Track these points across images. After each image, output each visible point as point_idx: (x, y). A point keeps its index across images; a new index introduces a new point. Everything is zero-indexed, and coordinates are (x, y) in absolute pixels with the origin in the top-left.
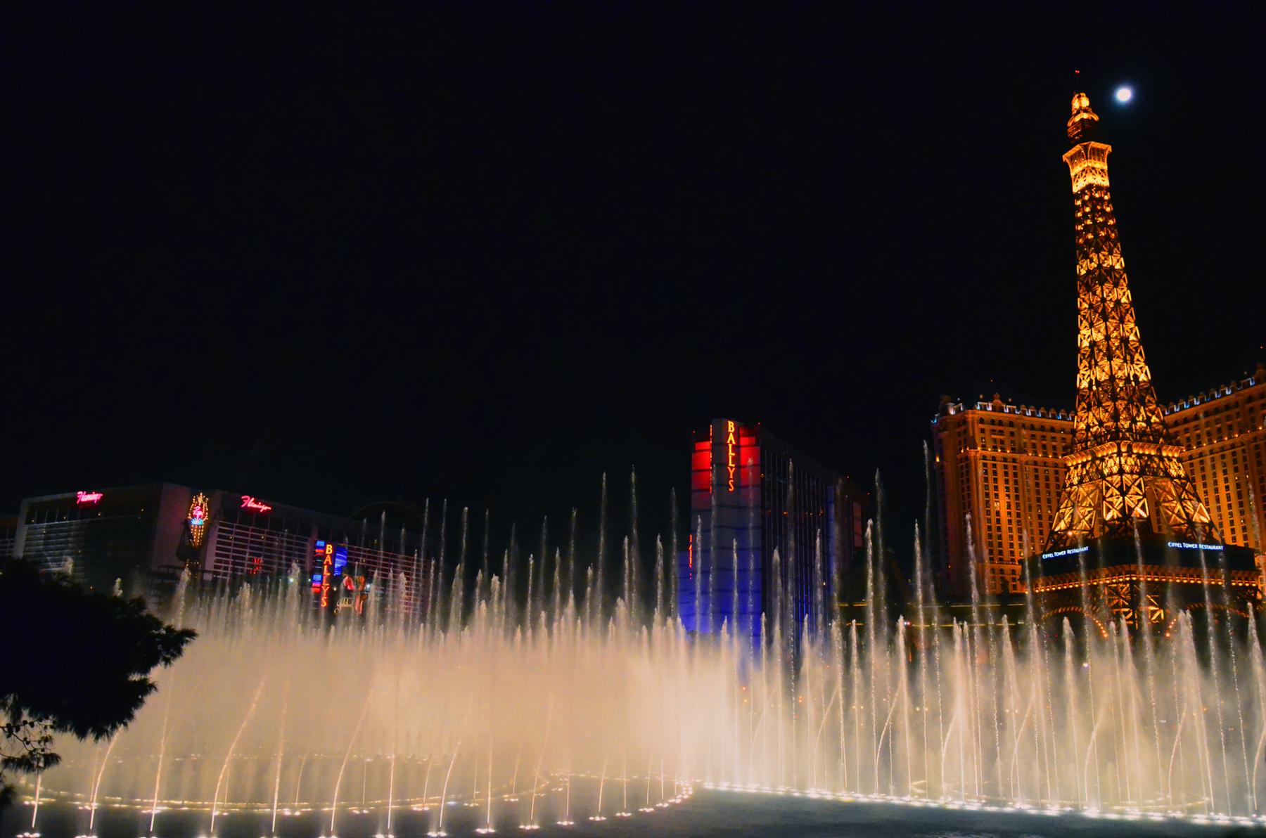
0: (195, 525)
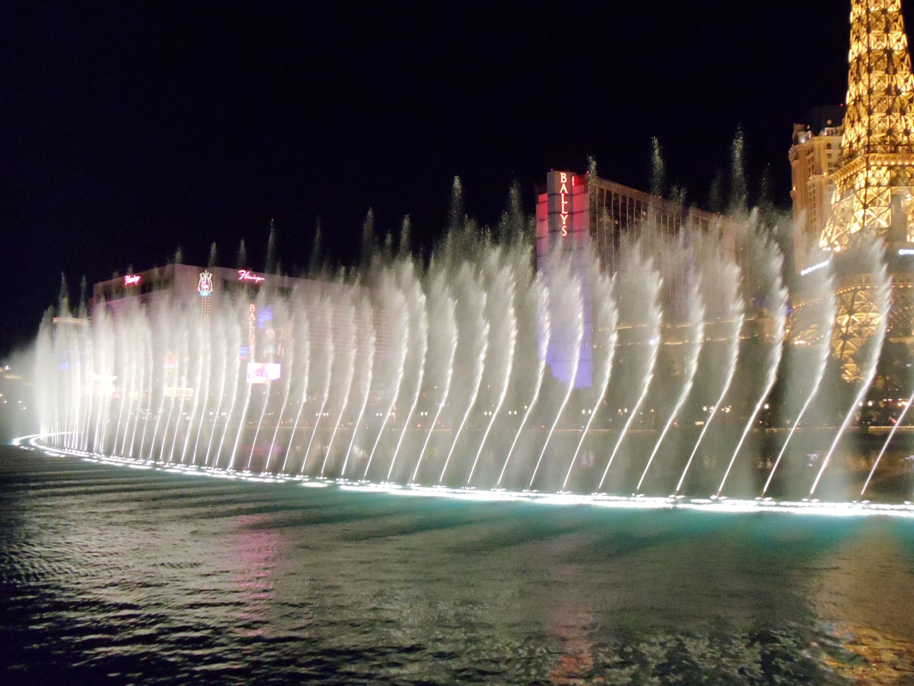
0: (204, 297)
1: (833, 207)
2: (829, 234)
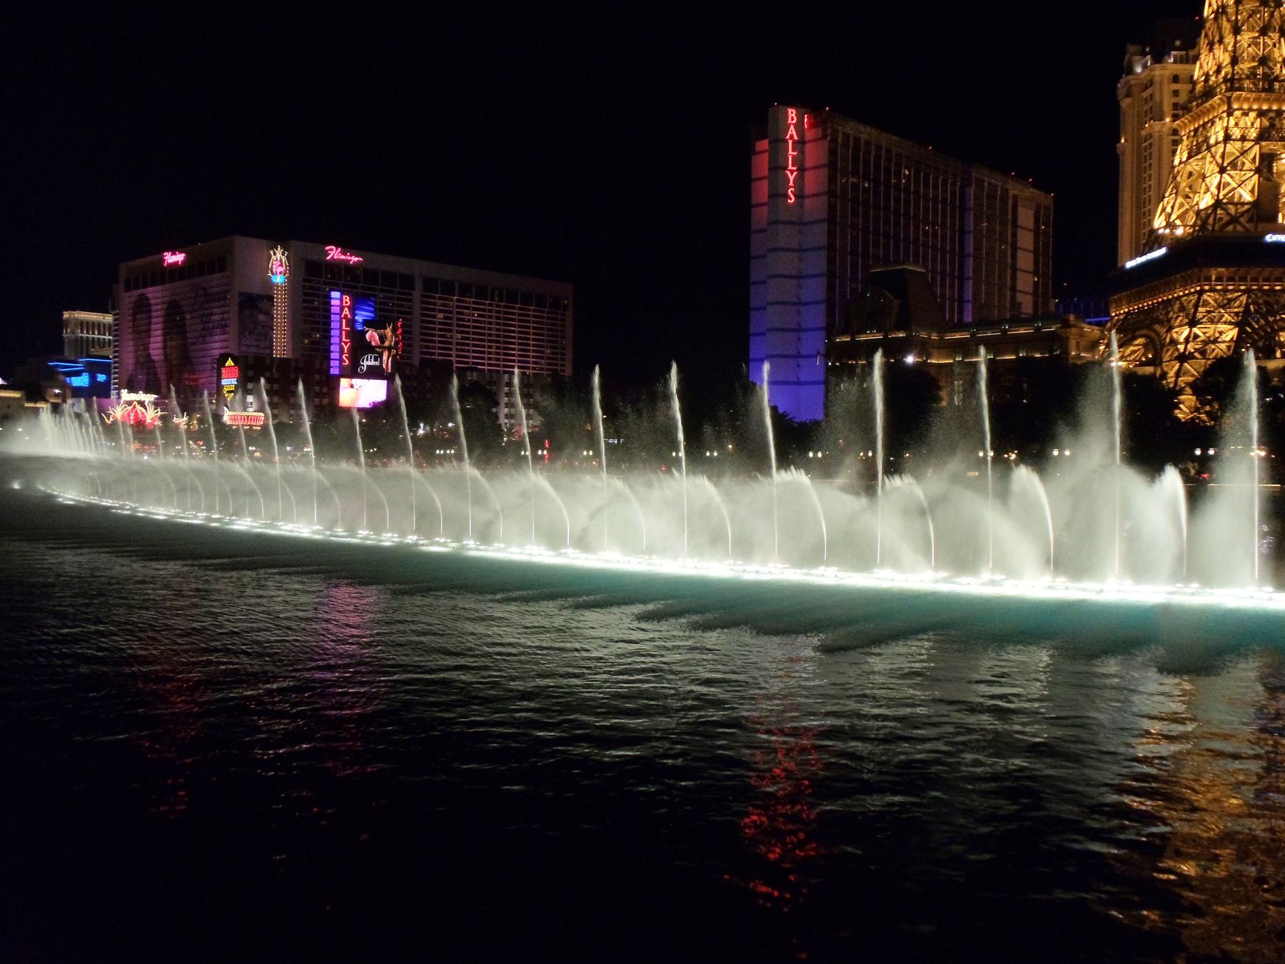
1: (1176, 170)
2: (1169, 210)
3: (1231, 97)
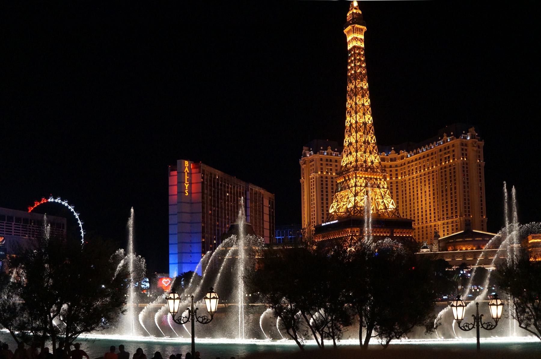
3: (356, 173)
